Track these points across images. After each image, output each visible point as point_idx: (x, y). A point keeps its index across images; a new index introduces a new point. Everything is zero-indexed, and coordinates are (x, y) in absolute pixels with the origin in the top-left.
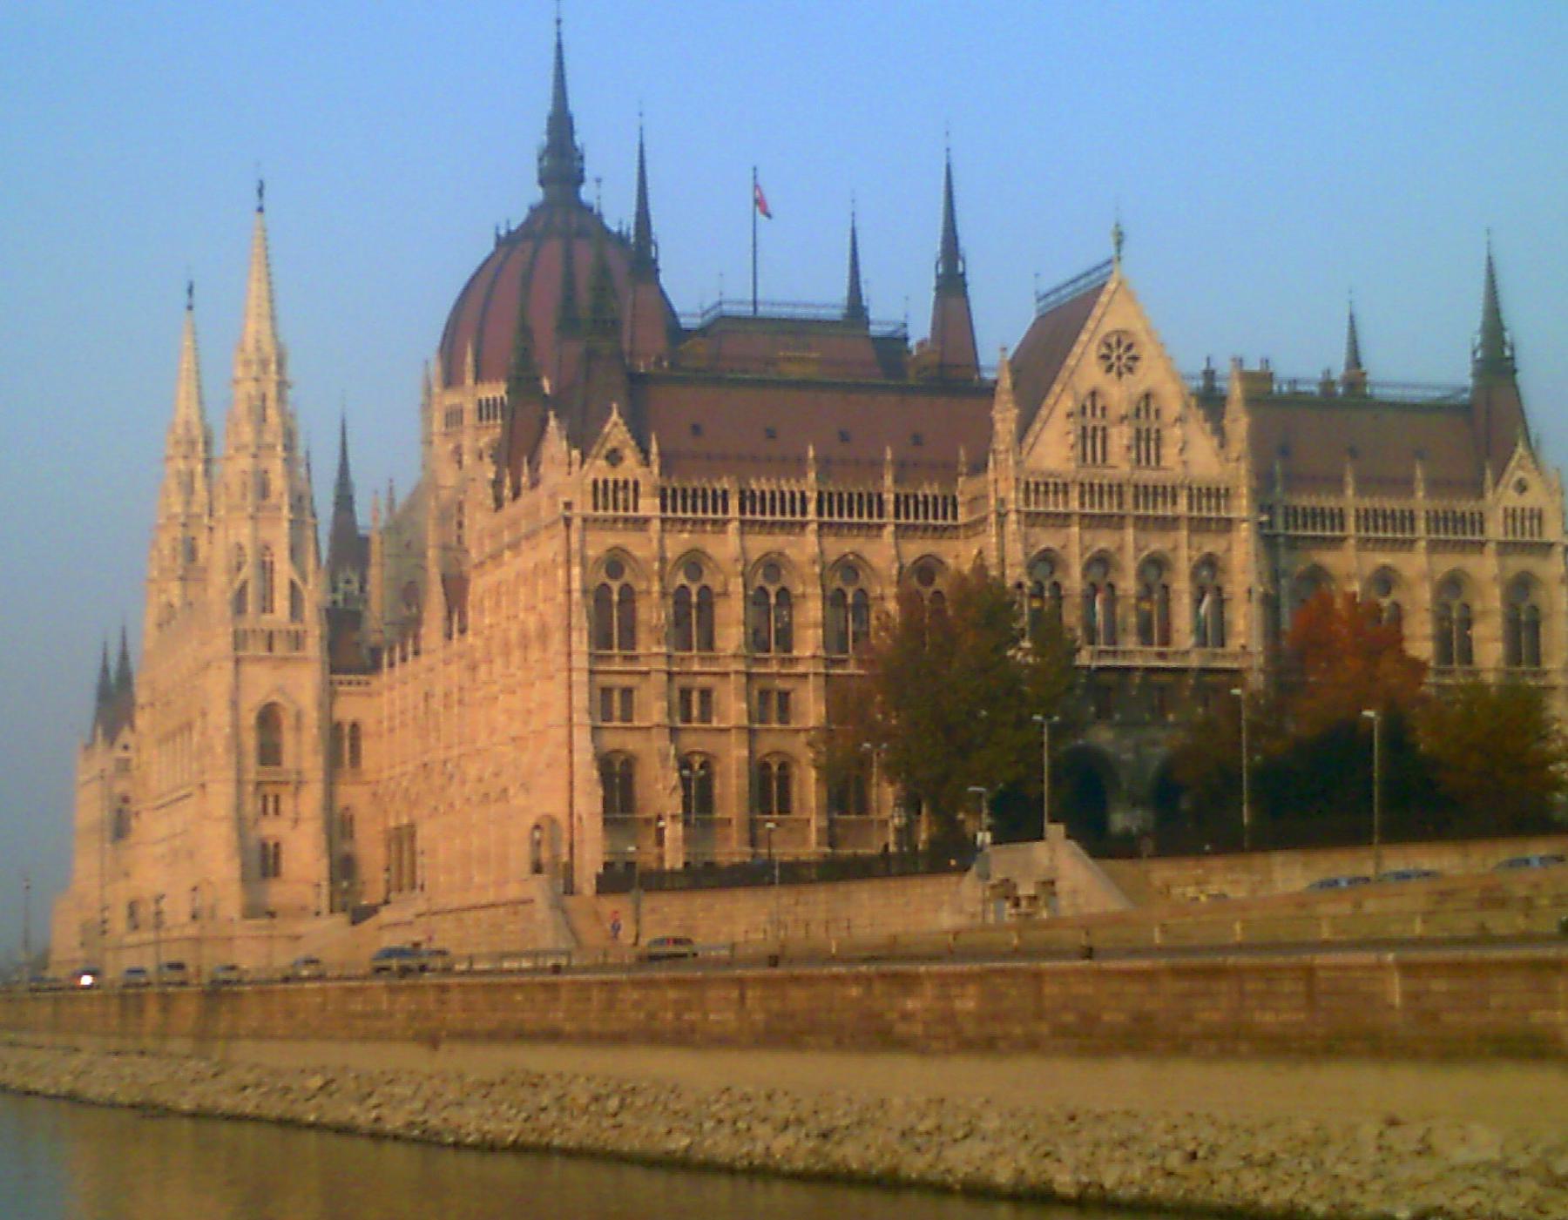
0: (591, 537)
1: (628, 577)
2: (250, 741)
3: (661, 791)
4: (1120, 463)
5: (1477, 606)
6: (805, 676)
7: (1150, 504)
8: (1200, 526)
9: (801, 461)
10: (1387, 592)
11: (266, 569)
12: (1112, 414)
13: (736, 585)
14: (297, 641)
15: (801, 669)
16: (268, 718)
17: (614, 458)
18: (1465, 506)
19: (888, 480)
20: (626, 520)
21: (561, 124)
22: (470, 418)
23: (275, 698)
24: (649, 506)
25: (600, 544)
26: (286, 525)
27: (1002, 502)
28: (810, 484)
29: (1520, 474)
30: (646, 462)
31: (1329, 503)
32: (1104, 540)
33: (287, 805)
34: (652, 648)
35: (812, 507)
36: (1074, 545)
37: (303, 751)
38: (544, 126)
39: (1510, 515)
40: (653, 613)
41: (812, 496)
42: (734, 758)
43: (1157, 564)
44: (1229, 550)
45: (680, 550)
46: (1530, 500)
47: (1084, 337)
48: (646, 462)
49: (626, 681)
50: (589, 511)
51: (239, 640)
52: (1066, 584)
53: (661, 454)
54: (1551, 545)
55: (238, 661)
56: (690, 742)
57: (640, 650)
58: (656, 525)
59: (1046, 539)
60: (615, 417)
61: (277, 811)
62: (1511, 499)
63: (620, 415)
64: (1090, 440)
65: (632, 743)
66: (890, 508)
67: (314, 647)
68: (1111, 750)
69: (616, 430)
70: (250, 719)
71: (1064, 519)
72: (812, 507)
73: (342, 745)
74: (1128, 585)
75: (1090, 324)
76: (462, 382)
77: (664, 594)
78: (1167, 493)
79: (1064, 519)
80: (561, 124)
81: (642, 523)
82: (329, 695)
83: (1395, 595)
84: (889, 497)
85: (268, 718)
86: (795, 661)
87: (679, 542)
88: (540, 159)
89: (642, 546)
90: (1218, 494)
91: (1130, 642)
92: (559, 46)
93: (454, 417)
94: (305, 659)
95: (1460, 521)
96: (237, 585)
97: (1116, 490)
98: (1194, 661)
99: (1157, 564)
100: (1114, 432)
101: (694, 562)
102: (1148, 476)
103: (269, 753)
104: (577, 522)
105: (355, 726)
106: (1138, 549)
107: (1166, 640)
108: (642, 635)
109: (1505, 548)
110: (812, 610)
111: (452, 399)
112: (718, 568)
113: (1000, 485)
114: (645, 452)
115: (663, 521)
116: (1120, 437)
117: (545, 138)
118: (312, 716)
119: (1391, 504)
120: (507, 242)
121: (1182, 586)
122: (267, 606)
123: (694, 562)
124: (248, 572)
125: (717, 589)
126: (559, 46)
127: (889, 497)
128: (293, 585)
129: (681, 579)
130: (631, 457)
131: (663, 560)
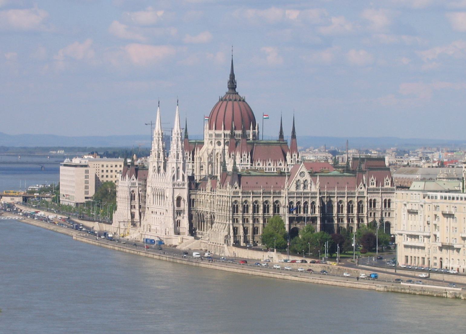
0: (233, 199)
1: (237, 204)
2: (175, 202)
3: (241, 232)
4: (301, 190)
5: (354, 205)
6: (260, 217)
7: (305, 195)
8: (312, 197)
9: (261, 187)
10: (341, 203)
11: (178, 172)
12: (301, 183)
13: (251, 205)
14: (184, 185)
15: (260, 215)
16: (179, 199)
17: (236, 188)
18: (352, 191)
19: (272, 190)
20: (237, 196)
21: (232, 76)
22: (214, 137)
23: (180, 195)
24: (240, 195)
25: (234, 199)
26: (182, 164)
27: (286, 195)
28: (262, 191)
29: (361, 186)
30: (240, 189)
31: (333, 191)
32: (299, 200)
33: (182, 215)
34: (240, 213)
35: (262, 194)
36: (295, 201)
37: (184, 206)
38: (229, 76)
39: (359, 192)
40: (240, 209)
41: (262, 193)
42: (250, 228)
43: (306, 203)
44: (316, 201)
45: (244, 200)
46: (362, 190)
47: (298, 172)
48: (240, 189)
49: (237, 218)
50: (232, 195)
51: (174, 185)
52: (294, 206)
53: (242, 187)
54: (365, 197)
55: (173, 189)
56: (245, 226)
57: (239, 213)
58: (241, 197)
59: (291, 200)
60: (236, 183)
61: (180, 215)
62: (360, 190)
63: (237, 182)
64: (297, 187)
65: (237, 226)
66: (272, 194)
67: (186, 186)
68: (299, 227)
69: (236, 184)
70: (175, 199)
71: (294, 197)
72: (262, 194)
73: (191, 202)
74: (302, 205)
75: (298, 171)
76: (213, 129)
77: (242, 206)
78: (308, 193)
79: (294, 197)
80: (232, 76)
81: (239, 197)
82: (189, 195)
83: (342, 204)
84: (272, 192)
85: (179, 199)
86: (259, 214)
87: (244, 199)
88: (228, 83)
89: (239, 200)
90: (315, 193)
91: (302, 213)
92: (232, 60)
93: (211, 135)
94: (185, 188)
95: (352, 193)
96: (173, 175)
97: (301, 193)
98: (310, 216)
99: (306, 203)
100: (301, 185)
101: (246, 202)
102: (305, 191)
103: (179, 205)
104: (231, 197)
105: (193, 200)
106: (304, 201)
107: (307, 213)
108: (239, 212)
109: (358, 197)
110: (261, 208)
111: (211, 132)
112: (249, 203)
113: (284, 193)
114: (240, 186)
115: (242, 196)
116: (302, 186)
117: (229, 79)
118: (186, 199)
119: (342, 191)
120: (221, 100)
121: (309, 205)
122: (178, 178)
123: (246, 202)
124: (175, 172)
125: (249, 205)
126: (232, 60)
127: (272, 192)
128: (183, 175)
129: (244, 204)
130: (238, 188)
131: (242, 202)
